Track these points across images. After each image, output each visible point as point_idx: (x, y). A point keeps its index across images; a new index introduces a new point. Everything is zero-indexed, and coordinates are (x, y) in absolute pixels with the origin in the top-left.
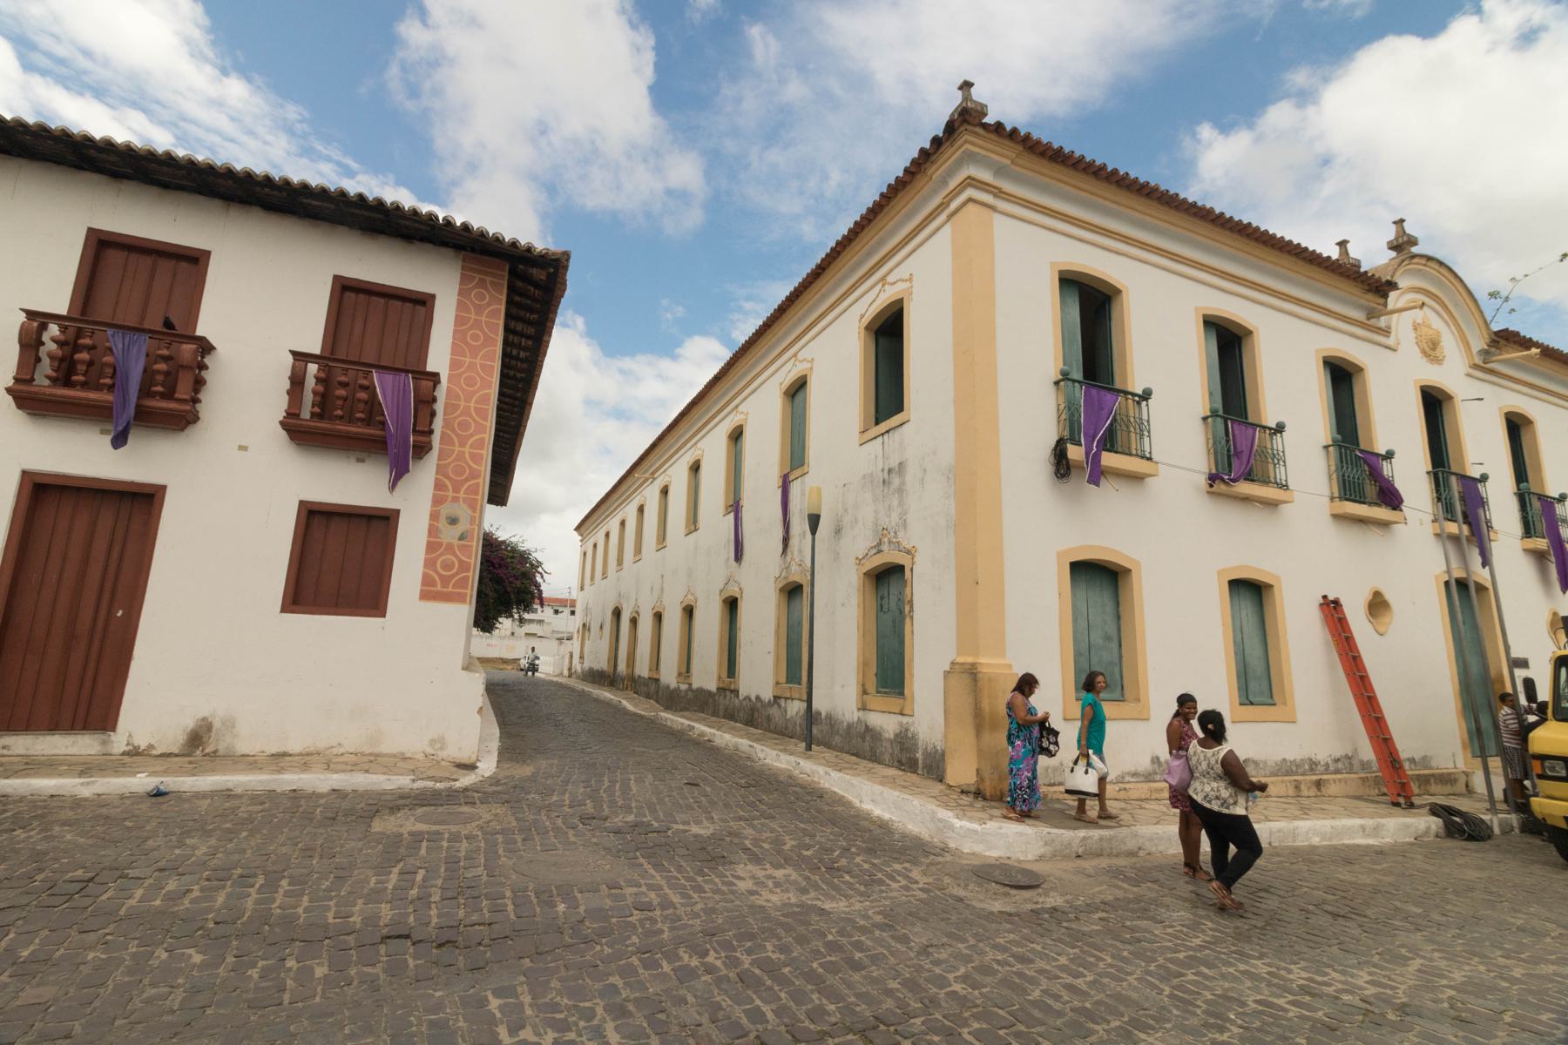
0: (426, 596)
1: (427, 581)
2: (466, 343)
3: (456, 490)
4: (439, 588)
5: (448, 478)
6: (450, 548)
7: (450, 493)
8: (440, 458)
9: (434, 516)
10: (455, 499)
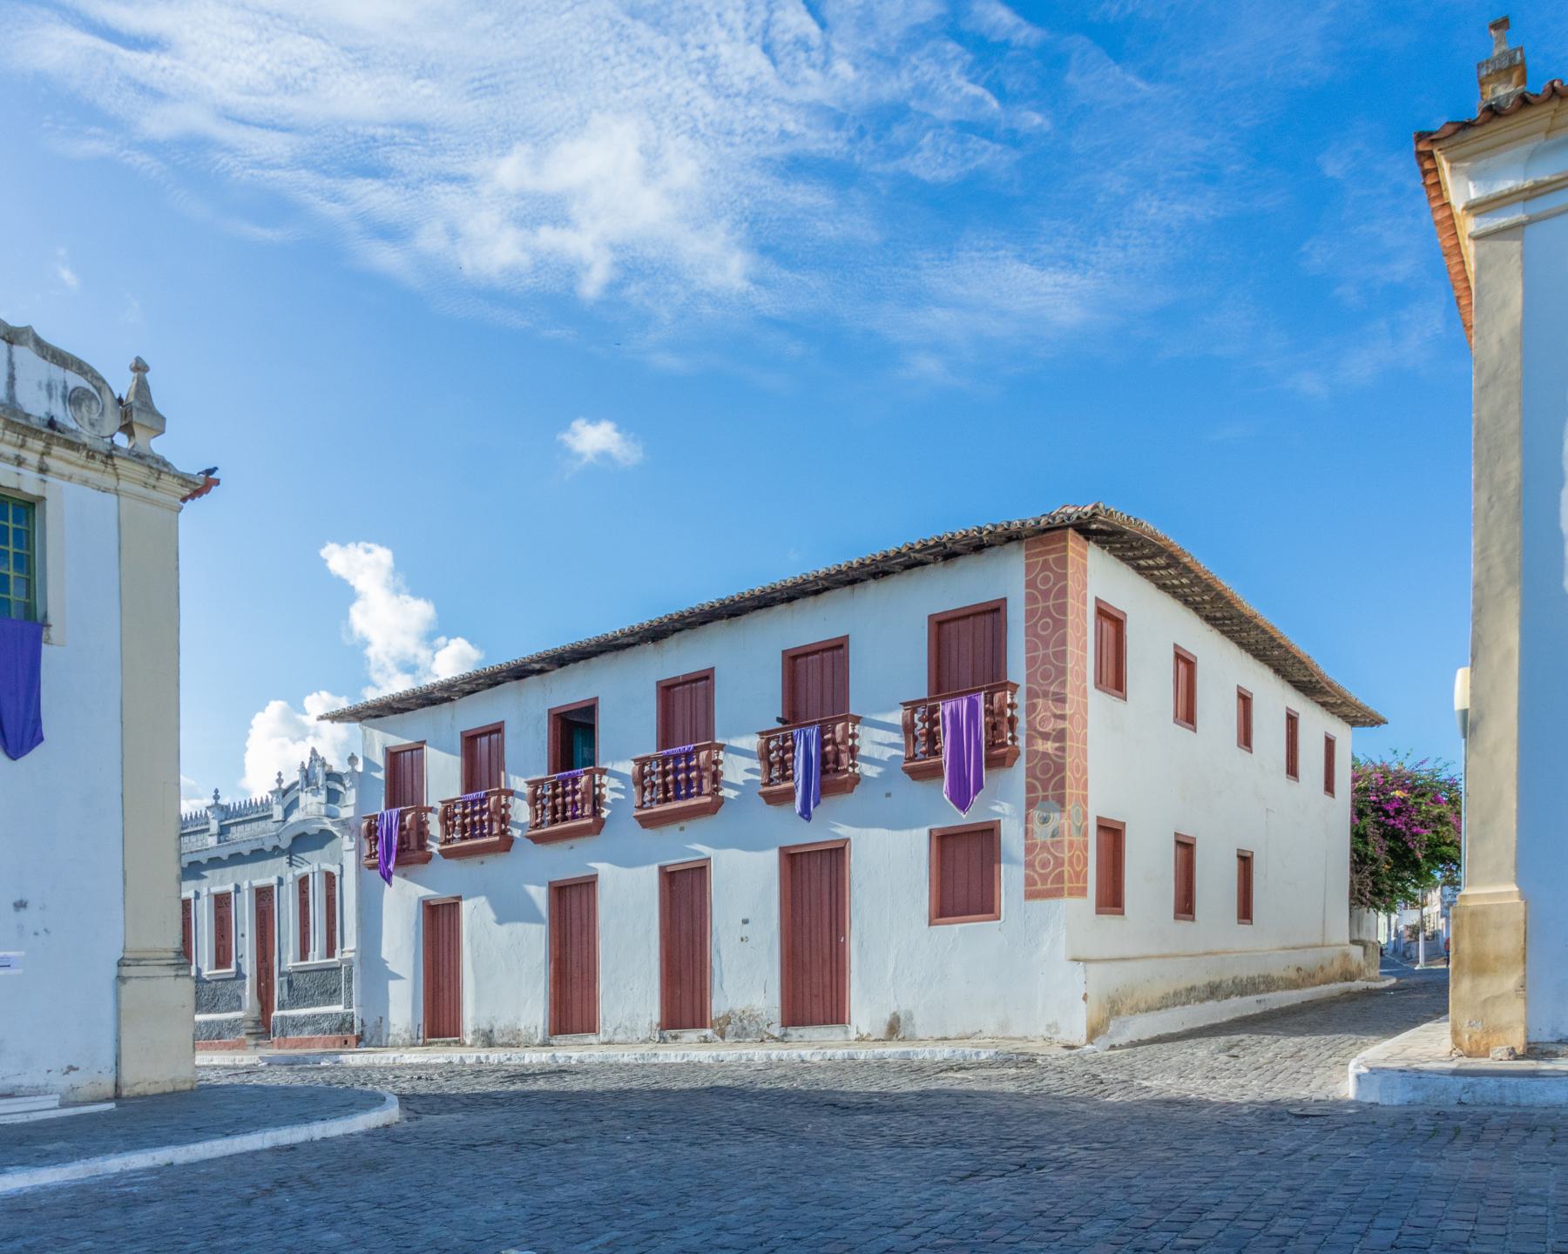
1: (1029, 881)
2: (1036, 635)
3: (1045, 789)
4: (1039, 886)
6: (1044, 847)
7: (1041, 793)
8: (1028, 761)
10: (1045, 798)
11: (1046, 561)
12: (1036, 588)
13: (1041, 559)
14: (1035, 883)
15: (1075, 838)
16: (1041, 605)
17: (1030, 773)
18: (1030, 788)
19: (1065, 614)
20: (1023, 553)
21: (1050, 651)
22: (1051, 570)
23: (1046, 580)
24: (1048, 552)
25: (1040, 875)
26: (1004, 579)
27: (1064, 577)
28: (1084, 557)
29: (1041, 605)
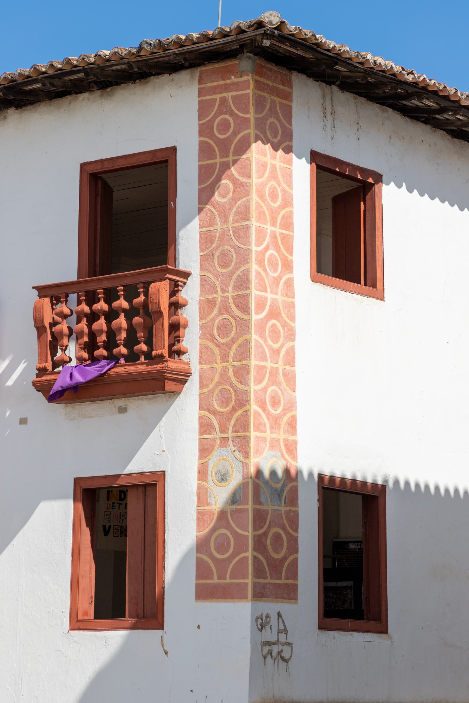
3: (223, 430)
4: (215, 580)
5: (214, 413)
7: (218, 435)
9: (203, 474)
11: (223, 101)
12: (212, 136)
15: (269, 507)
17: (204, 405)
18: (205, 427)
21: (230, 225)
22: (232, 114)
23: (225, 126)
24: (227, 88)
28: (288, 97)
29: (219, 160)
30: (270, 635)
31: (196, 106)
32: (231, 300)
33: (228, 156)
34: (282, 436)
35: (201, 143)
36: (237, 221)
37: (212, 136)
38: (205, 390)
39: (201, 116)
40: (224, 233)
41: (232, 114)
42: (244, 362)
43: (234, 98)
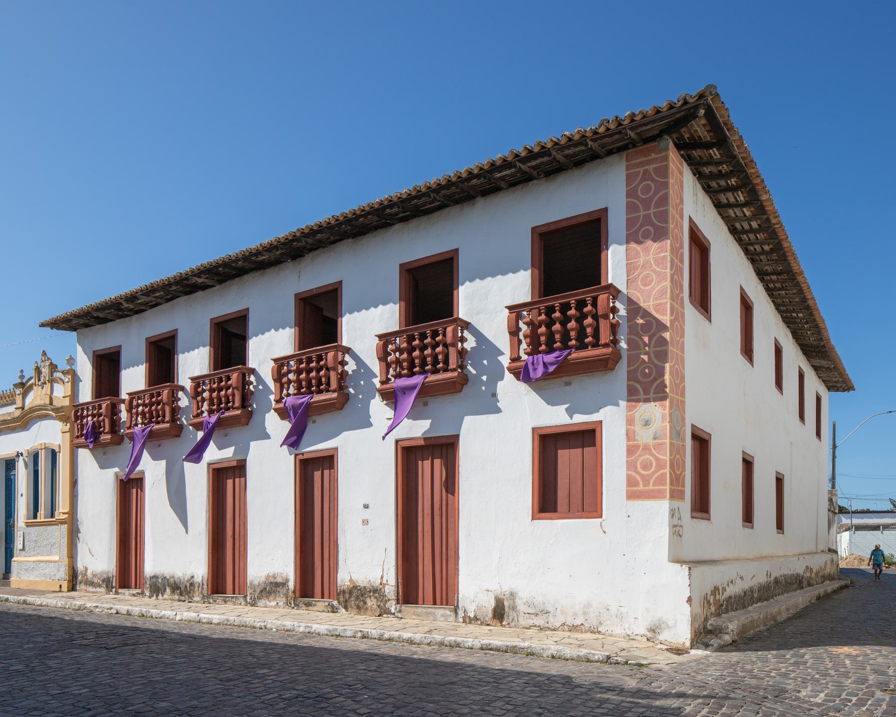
0: (632, 496)
1: (631, 482)
4: (641, 487)
5: (639, 382)
6: (646, 448)
8: (629, 366)
12: (638, 198)
13: (642, 169)
14: (636, 484)
16: (642, 213)
17: (631, 376)
19: (666, 221)
20: (623, 165)
23: (647, 189)
24: (649, 162)
25: (642, 476)
26: (603, 190)
27: (666, 185)
29: (642, 213)
30: (676, 522)
31: (624, 177)
32: (651, 307)
33: (649, 209)
34: (680, 398)
35: (627, 203)
36: (658, 253)
37: (638, 198)
38: (632, 368)
39: (627, 185)
40: (647, 262)
41: (653, 180)
42: (663, 348)
43: (655, 169)
